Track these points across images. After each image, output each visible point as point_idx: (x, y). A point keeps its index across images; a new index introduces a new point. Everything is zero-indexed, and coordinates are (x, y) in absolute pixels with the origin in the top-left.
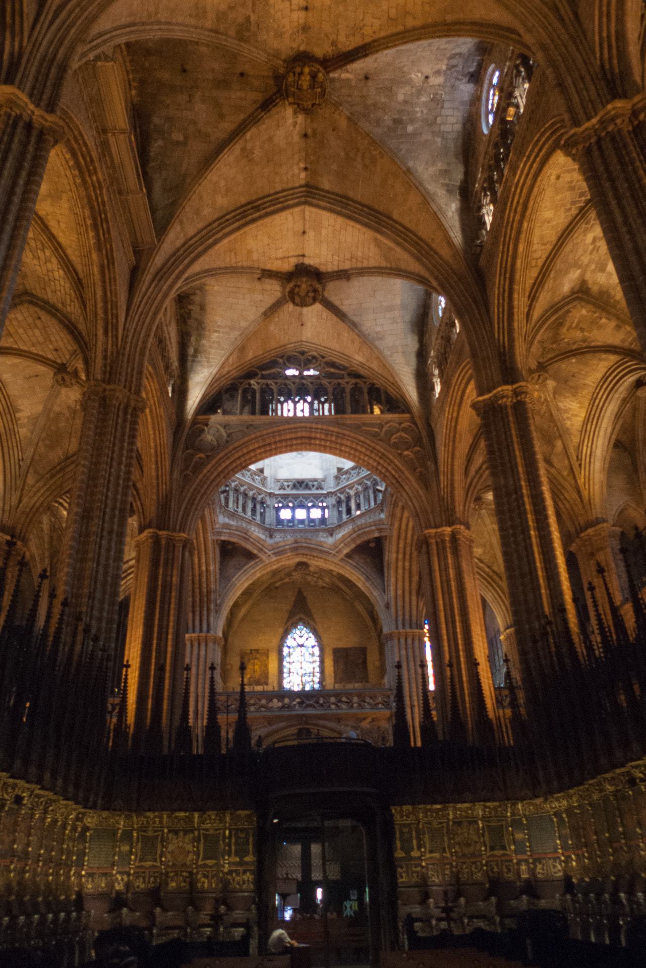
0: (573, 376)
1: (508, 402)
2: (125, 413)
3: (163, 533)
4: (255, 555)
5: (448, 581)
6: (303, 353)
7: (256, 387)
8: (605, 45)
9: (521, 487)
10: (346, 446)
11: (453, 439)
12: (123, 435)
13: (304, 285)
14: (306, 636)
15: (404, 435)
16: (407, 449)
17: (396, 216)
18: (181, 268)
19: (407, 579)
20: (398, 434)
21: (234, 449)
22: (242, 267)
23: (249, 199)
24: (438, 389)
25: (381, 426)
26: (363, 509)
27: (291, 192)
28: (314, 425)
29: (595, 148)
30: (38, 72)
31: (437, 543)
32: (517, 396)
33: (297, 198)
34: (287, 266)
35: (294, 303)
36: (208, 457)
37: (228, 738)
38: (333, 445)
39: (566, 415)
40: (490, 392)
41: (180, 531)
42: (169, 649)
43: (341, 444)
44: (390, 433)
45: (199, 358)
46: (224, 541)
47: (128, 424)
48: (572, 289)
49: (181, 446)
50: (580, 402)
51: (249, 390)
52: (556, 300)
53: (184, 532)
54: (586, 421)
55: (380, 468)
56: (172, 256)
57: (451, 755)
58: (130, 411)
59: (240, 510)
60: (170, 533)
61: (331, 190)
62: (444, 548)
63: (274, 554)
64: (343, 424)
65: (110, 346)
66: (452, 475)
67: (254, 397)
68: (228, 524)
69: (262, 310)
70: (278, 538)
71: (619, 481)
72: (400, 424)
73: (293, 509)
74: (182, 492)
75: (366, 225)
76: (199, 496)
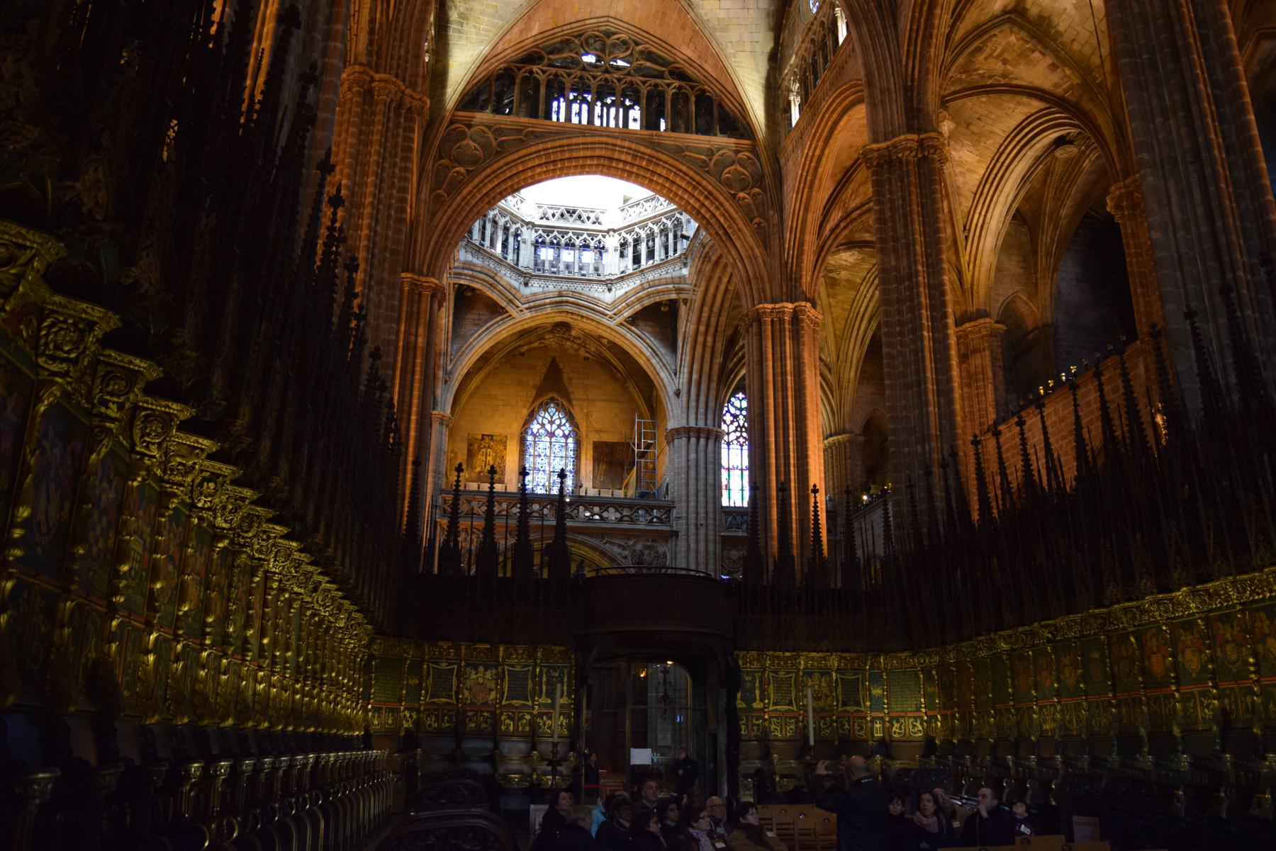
1: (910, 156)
2: (398, 115)
5: (784, 374)
6: (609, 34)
9: (917, 272)
10: (660, 175)
11: (809, 184)
12: (395, 145)
14: (558, 422)
15: (739, 168)
16: (742, 190)
19: (707, 359)
21: (506, 164)
25: (711, 153)
26: (657, 257)
28: (619, 142)
31: (772, 321)
32: (923, 151)
37: (470, 550)
39: (958, 170)
40: (886, 140)
41: (427, 275)
42: (412, 433)
43: (654, 173)
44: (722, 164)
45: (465, 28)
46: (461, 285)
47: (401, 131)
48: (1005, 7)
49: (434, 152)
50: (980, 155)
51: (530, 81)
52: (983, 18)
53: (433, 276)
54: (984, 181)
55: (703, 211)
57: (766, 588)
59: (487, 243)
62: (782, 330)
63: (529, 308)
64: (659, 144)
65: (378, 16)
66: (803, 233)
67: (537, 92)
68: (471, 263)
70: (536, 287)
71: (1013, 265)
72: (737, 152)
74: (432, 219)
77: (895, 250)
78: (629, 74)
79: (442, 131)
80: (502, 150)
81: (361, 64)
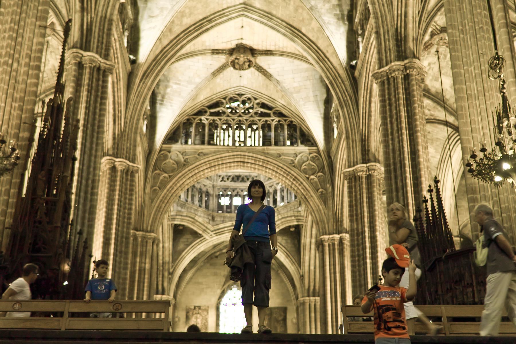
0: (429, 133)
3: (140, 233)
4: (200, 234)
5: (335, 273)
7: (206, 122)
8: (399, 18)
9: (365, 231)
10: (270, 169)
12: (126, 189)
13: (242, 58)
16: (313, 174)
17: (304, 31)
18: (159, 68)
20: (307, 163)
21: (189, 170)
22: (199, 51)
23: (204, 16)
24: (336, 132)
26: (286, 201)
27: (233, 8)
28: (247, 154)
29: (386, 82)
30: (99, 29)
31: (329, 245)
33: (238, 12)
34: (232, 45)
35: (234, 68)
36: (170, 176)
38: (260, 168)
41: (150, 232)
43: (266, 168)
45: (165, 102)
49: (151, 168)
54: (441, 162)
56: (154, 60)
58: (129, 173)
59: (190, 199)
60: (144, 233)
61: (261, 8)
62: (334, 249)
64: (268, 154)
69: (212, 71)
73: (231, 197)
74: (152, 202)
75: (284, 35)
76: (164, 205)
77: (357, 220)
78: (252, 116)
79: (155, 157)
80: (186, 163)
81: (110, 155)
